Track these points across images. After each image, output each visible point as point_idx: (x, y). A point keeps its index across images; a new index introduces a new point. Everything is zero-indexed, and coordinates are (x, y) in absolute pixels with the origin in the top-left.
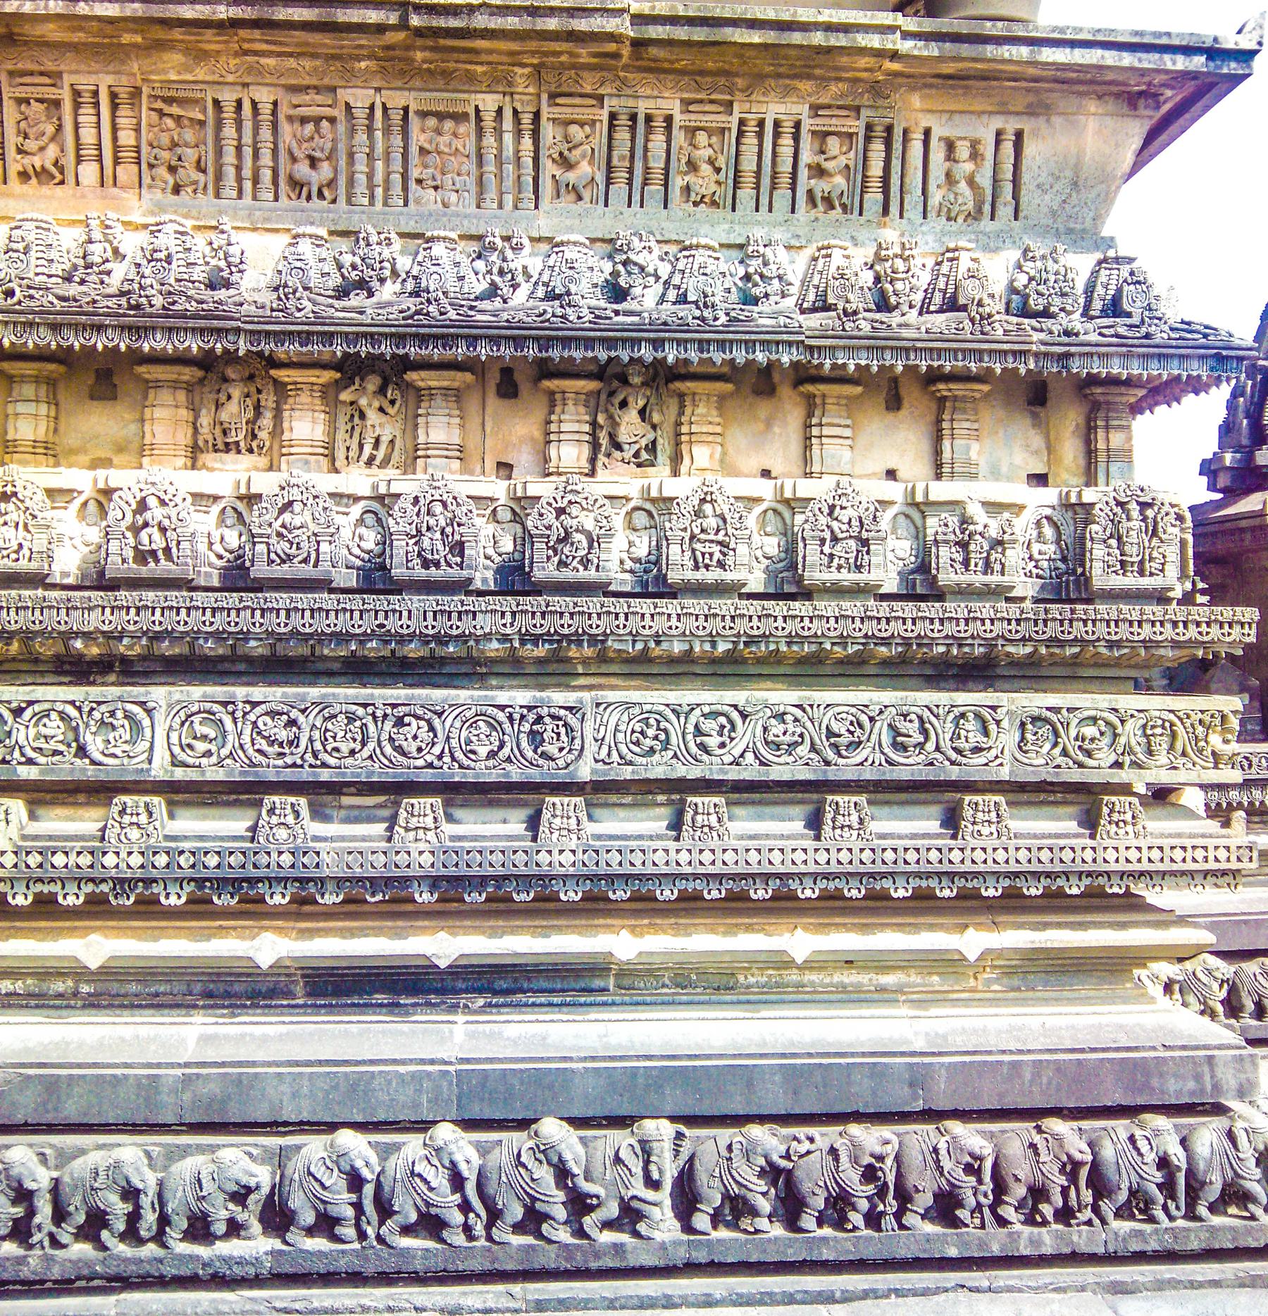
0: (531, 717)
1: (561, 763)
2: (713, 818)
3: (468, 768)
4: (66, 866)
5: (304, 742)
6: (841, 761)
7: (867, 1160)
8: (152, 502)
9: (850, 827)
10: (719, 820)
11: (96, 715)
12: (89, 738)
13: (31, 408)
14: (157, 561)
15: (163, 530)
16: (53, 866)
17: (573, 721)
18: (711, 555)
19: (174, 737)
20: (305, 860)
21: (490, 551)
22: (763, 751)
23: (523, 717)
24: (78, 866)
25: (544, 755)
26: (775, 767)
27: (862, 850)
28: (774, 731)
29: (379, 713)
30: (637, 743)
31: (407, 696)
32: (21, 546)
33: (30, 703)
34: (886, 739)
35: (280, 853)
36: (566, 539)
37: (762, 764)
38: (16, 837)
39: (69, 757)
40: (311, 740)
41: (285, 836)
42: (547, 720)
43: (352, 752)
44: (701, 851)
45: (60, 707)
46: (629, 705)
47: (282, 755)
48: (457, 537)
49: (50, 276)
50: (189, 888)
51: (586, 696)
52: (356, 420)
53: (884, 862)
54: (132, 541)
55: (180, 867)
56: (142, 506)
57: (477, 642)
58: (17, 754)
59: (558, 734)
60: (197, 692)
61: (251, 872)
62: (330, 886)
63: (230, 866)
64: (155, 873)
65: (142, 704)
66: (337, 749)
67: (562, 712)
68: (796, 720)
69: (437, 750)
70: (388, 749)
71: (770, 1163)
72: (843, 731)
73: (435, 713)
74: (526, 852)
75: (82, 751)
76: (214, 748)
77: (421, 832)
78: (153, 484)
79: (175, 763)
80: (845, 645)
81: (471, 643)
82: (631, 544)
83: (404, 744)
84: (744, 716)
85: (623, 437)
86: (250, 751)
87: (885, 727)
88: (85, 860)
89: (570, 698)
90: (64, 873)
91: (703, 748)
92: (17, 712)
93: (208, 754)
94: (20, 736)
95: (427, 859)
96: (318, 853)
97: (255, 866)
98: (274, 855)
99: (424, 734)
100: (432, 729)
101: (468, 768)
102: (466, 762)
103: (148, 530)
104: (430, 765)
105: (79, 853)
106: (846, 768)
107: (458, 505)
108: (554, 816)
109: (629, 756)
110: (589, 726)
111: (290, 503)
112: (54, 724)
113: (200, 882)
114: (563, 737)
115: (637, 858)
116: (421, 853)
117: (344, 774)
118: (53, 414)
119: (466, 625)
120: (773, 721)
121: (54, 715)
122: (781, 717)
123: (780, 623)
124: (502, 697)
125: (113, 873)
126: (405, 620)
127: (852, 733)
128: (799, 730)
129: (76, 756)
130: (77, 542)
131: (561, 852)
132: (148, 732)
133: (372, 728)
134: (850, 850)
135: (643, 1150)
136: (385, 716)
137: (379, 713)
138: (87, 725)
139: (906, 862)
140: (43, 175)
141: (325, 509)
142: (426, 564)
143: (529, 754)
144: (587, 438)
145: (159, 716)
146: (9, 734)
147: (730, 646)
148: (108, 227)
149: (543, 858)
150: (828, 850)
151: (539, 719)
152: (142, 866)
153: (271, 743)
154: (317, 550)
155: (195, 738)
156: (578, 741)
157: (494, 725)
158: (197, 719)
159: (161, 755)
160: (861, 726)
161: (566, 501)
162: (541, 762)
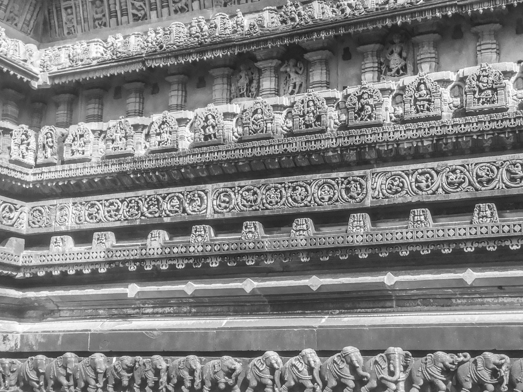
0: (346, 182)
1: (358, 200)
2: (422, 218)
3: (321, 205)
4: (177, 253)
5: (259, 200)
6: (483, 188)
7: (492, 366)
8: (210, 117)
9: (486, 217)
10: (425, 218)
11: (189, 196)
12: (187, 205)
13: (176, 93)
14: (211, 139)
15: (213, 127)
16: (174, 253)
17: (363, 181)
18: (423, 105)
19: (215, 202)
20: (258, 245)
21: (337, 121)
22: (446, 187)
23: (342, 183)
24: (182, 252)
25: (351, 197)
26: (452, 194)
27: (492, 227)
28: (451, 177)
29: (287, 186)
30: (390, 189)
31: (297, 178)
32: (168, 139)
33: (168, 194)
34: (505, 177)
35: (250, 243)
36: (362, 109)
37: (446, 193)
38: (162, 242)
39: (180, 213)
40: (262, 199)
41: (251, 236)
42: (352, 182)
43: (277, 203)
44: (417, 232)
45: (177, 194)
46: (386, 173)
47: (251, 206)
48: (318, 113)
49: (179, 43)
50: (219, 260)
51: (368, 171)
52: (288, 78)
53: (503, 232)
54: (203, 132)
55: (215, 251)
56: (207, 119)
57: (324, 153)
58: (164, 213)
59: (357, 188)
60: (222, 185)
61: (240, 251)
62: (269, 257)
63: (232, 249)
64: (207, 254)
65: (203, 191)
66: (271, 202)
67: (358, 178)
68: (461, 172)
69: (309, 199)
70: (290, 200)
71: (445, 366)
72: (484, 174)
73: (307, 183)
74: (343, 237)
75: (184, 211)
76: (228, 205)
77: (301, 232)
78: (210, 110)
79: (215, 212)
80: (482, 135)
81: (322, 154)
82: (395, 110)
83: (296, 197)
84: (438, 173)
85: (392, 66)
86: (240, 205)
87: (504, 172)
88: (184, 250)
89: (361, 172)
90: (177, 255)
91: (419, 188)
92: (164, 198)
93: (226, 208)
94: (165, 206)
95: (304, 242)
96: (263, 242)
97: (241, 249)
98: (248, 244)
99: (304, 193)
100: (307, 191)
101: (321, 205)
102: (320, 202)
103: (208, 127)
104: (306, 205)
105: (182, 247)
106: (485, 191)
107: (319, 100)
108: (354, 221)
109: (387, 194)
110: (370, 183)
111: (257, 109)
112: (176, 201)
113: (222, 256)
114: (359, 189)
115: (389, 237)
116: (301, 240)
117: (274, 212)
118: (184, 95)
119: (318, 146)
120: (451, 173)
121: (175, 198)
122: (454, 171)
123: (450, 128)
124: (334, 175)
125: (193, 254)
126: (294, 147)
127: (488, 175)
128: (462, 176)
129: (182, 213)
130: (189, 138)
131: (357, 236)
132: (206, 201)
133: (284, 192)
134: (486, 227)
135: (387, 358)
136: (289, 187)
137: (287, 186)
138: (186, 200)
139: (515, 231)
140: (182, 10)
141: (269, 110)
142: (307, 126)
143: (345, 197)
144: (377, 69)
145: (209, 194)
146: (162, 205)
147: (430, 143)
148: (200, 22)
149: (350, 239)
150: (476, 228)
151: (349, 183)
152: (202, 251)
153: (247, 202)
154: (266, 127)
155: (222, 202)
156: (365, 190)
157: (331, 186)
158: (222, 195)
159: (210, 211)
160: (492, 171)
161: (361, 93)
162: (350, 200)
